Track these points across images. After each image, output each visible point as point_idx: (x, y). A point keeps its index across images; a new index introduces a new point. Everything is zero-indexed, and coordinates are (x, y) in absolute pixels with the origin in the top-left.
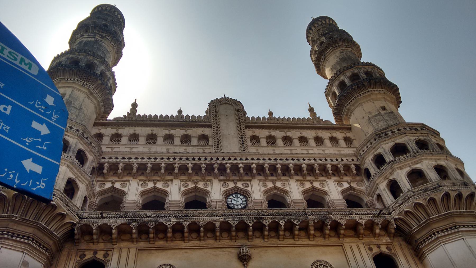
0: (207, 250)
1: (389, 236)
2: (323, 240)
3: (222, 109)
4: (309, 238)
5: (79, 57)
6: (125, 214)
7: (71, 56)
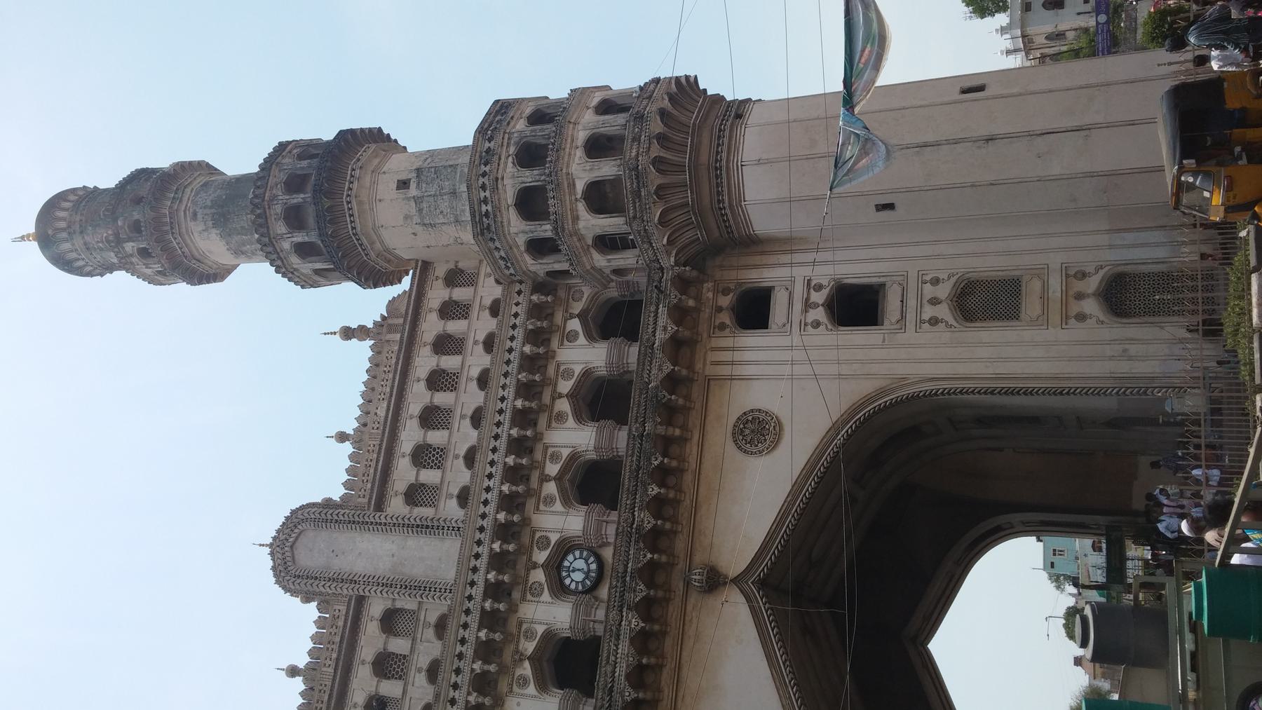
0: (685, 654)
1: (703, 282)
4: (686, 440)
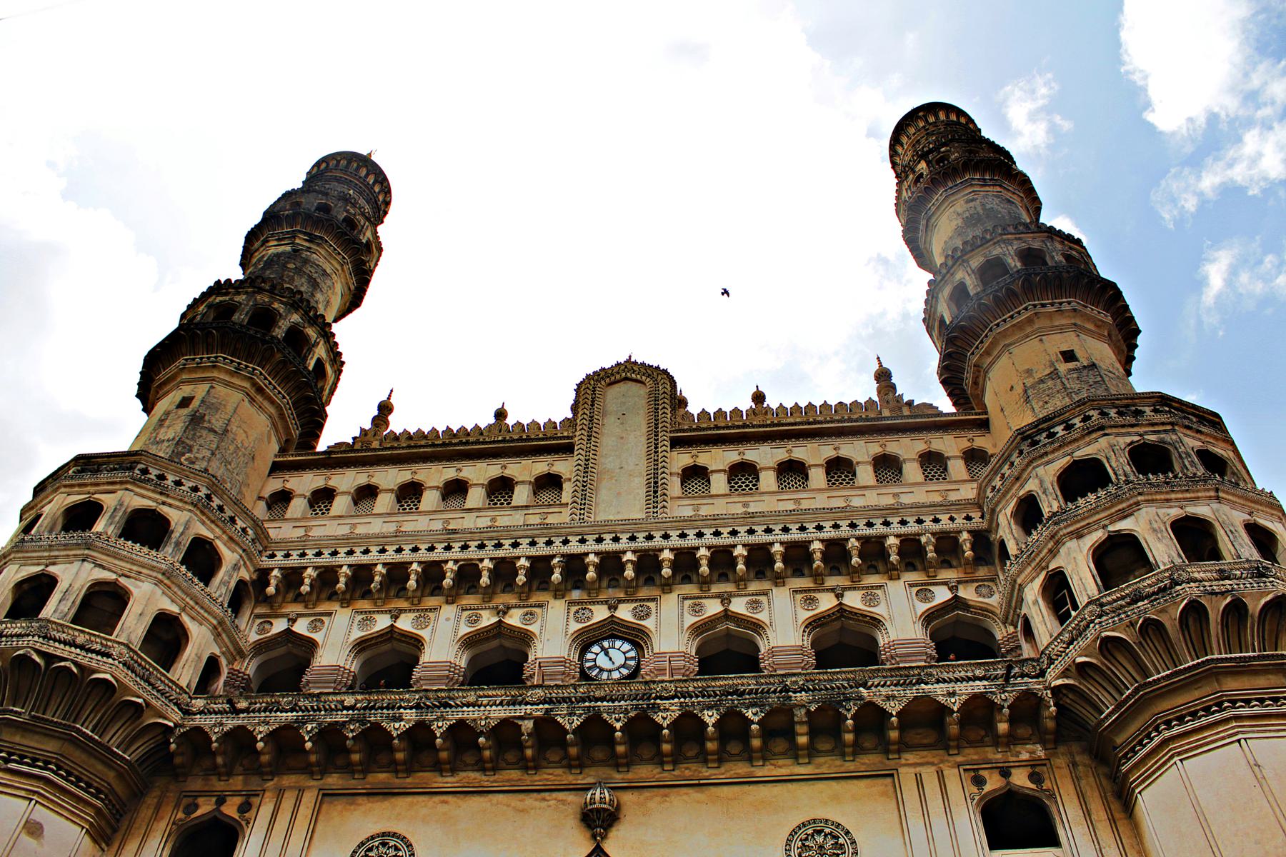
0: (501, 796)
1: (1043, 742)
2: (838, 762)
3: (613, 396)
4: (796, 757)
5: (237, 298)
6: (290, 703)
7: (219, 299)
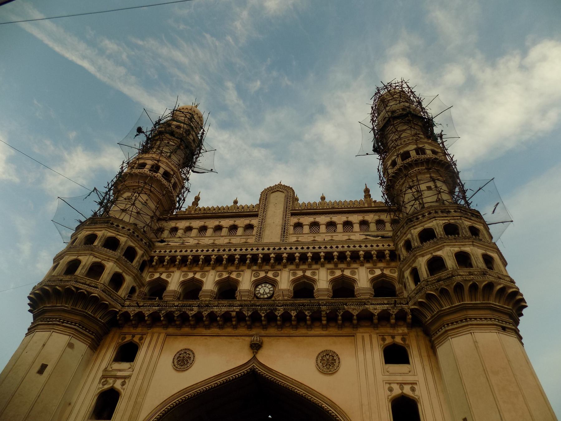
0: (224, 337)
1: (408, 327)
